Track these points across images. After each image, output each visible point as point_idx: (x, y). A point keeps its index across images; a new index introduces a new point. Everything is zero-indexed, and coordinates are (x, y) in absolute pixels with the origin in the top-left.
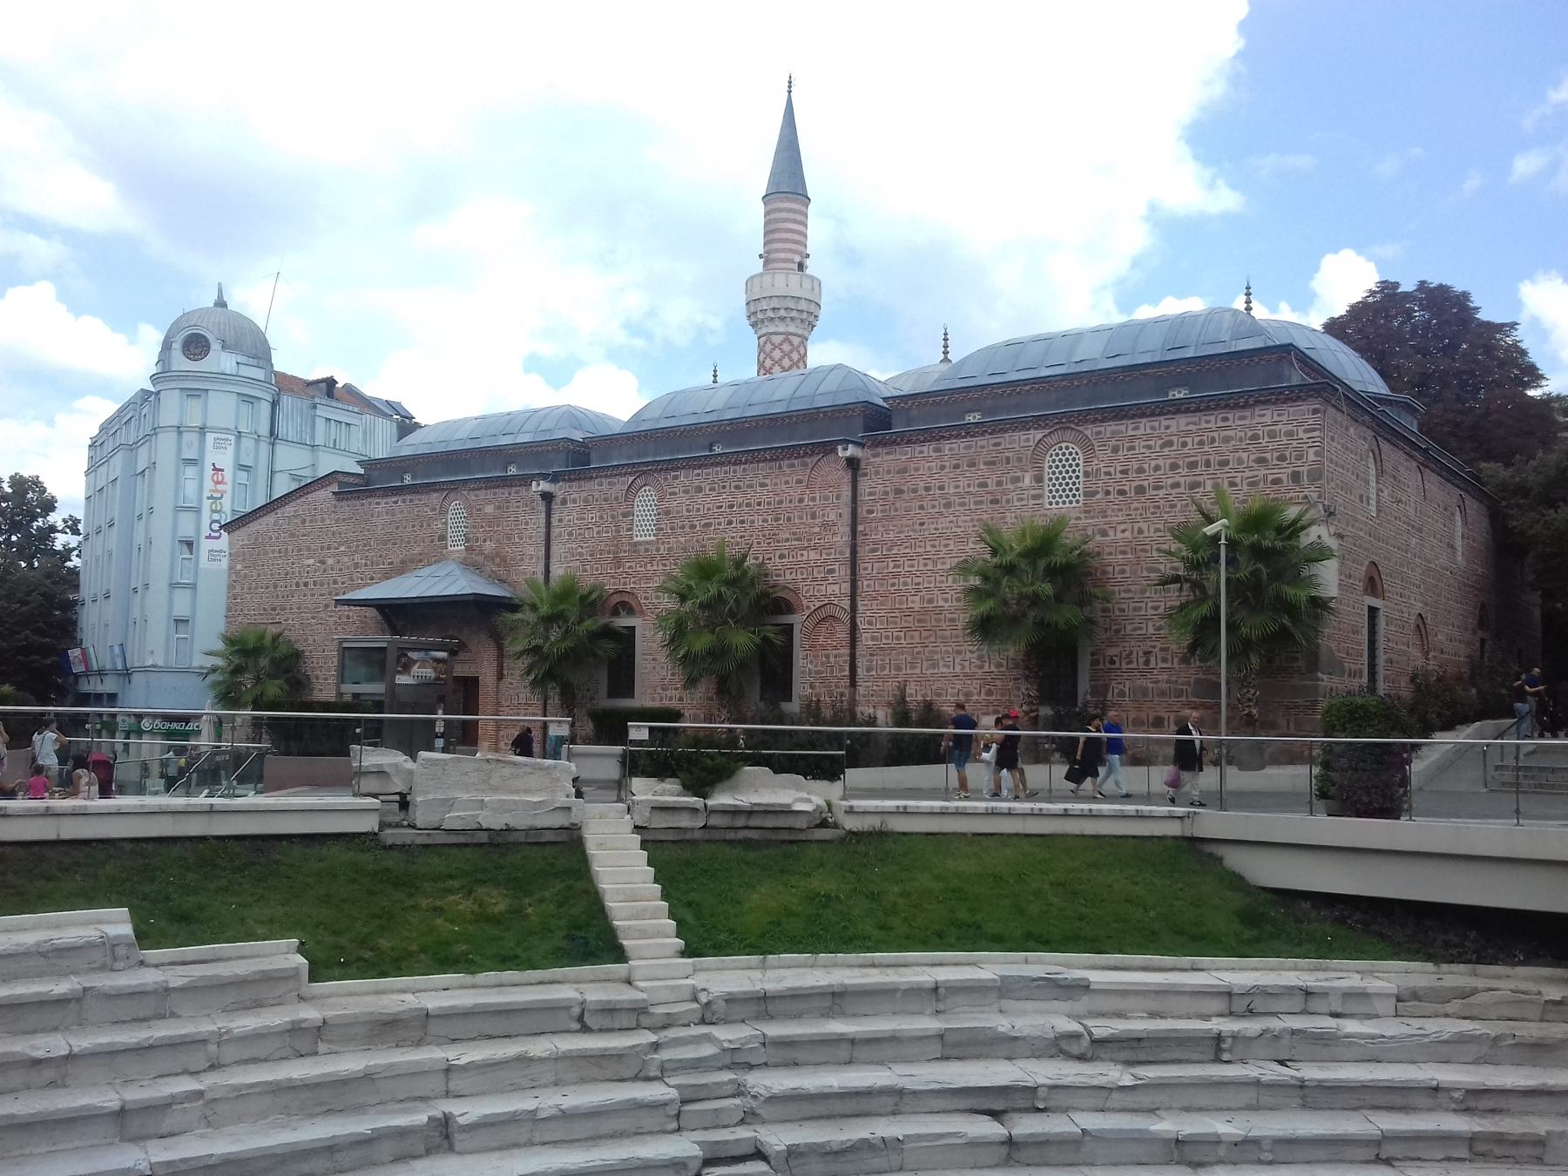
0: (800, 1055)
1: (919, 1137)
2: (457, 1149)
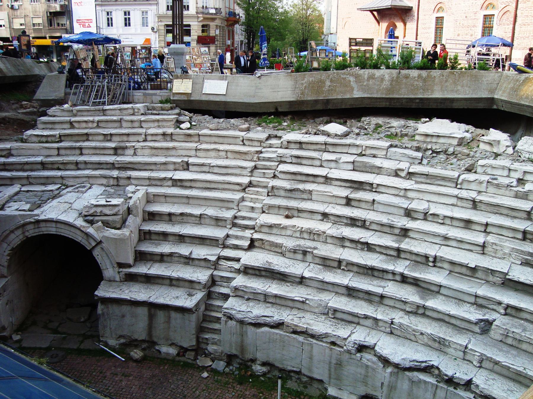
0: (304, 162)
1: (318, 191)
2: (190, 169)
